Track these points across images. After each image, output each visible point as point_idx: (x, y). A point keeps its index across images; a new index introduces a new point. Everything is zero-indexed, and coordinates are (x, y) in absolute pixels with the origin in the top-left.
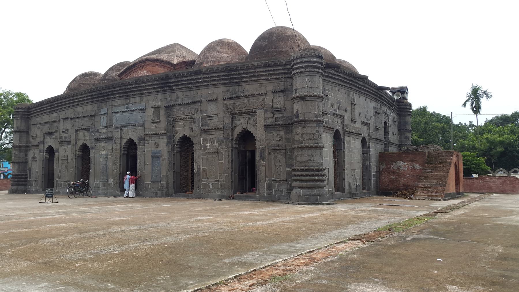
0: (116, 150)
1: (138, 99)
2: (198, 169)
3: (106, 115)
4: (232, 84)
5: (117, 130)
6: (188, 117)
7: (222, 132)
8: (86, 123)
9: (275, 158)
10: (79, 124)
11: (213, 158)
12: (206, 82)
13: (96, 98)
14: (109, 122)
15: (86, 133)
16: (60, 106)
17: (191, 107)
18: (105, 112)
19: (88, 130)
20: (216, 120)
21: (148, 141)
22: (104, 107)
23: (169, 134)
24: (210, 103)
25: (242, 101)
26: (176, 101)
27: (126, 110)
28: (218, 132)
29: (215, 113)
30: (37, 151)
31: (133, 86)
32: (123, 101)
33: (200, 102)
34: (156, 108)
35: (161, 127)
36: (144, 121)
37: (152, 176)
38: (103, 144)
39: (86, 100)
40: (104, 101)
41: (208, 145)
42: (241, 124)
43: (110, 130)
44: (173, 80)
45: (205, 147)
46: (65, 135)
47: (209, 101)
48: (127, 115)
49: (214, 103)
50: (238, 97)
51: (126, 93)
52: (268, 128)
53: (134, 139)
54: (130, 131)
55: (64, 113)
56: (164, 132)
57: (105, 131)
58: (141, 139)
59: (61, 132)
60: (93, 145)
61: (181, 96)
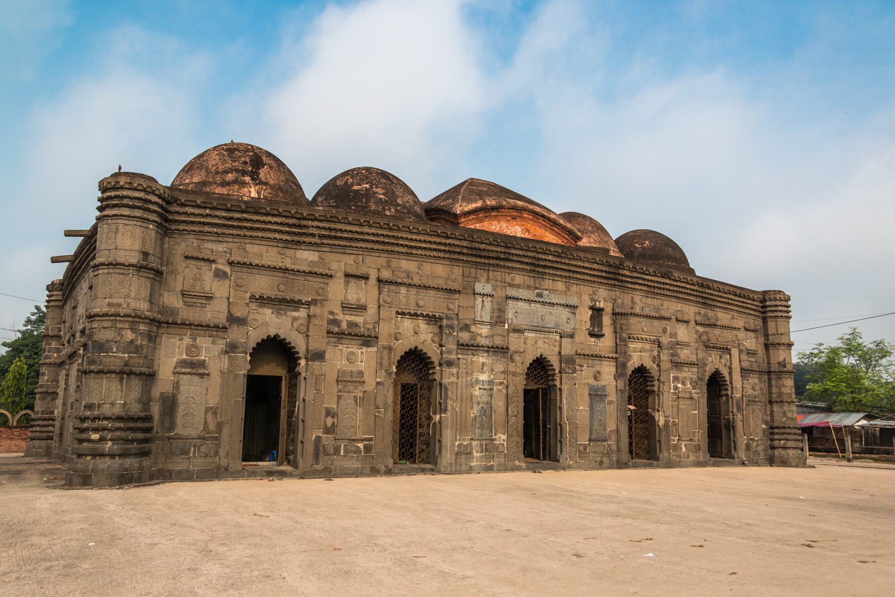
0: (514, 374)
1: (560, 285)
2: (667, 422)
3: (489, 299)
5: (516, 335)
6: (652, 338)
7: (696, 370)
8: (432, 303)
9: (753, 411)
11: (679, 406)
13: (463, 254)
14: (496, 314)
15: (422, 325)
16: (340, 238)
17: (656, 323)
18: (488, 289)
20: (688, 352)
21: (581, 366)
23: (621, 359)
24: (680, 324)
25: (717, 331)
26: (632, 308)
27: (541, 300)
28: (692, 369)
29: (686, 339)
30: (209, 350)
31: (550, 257)
32: (531, 282)
33: (668, 319)
35: (606, 344)
37: (591, 433)
38: (481, 360)
40: (485, 267)
41: (679, 385)
42: (714, 362)
44: (628, 273)
45: (676, 388)
47: (677, 320)
50: (714, 326)
51: (538, 266)
52: (745, 372)
53: (549, 358)
54: (540, 343)
55: (350, 259)
56: (611, 355)
57: (485, 330)
58: (569, 361)
59: (337, 310)
60: (453, 356)
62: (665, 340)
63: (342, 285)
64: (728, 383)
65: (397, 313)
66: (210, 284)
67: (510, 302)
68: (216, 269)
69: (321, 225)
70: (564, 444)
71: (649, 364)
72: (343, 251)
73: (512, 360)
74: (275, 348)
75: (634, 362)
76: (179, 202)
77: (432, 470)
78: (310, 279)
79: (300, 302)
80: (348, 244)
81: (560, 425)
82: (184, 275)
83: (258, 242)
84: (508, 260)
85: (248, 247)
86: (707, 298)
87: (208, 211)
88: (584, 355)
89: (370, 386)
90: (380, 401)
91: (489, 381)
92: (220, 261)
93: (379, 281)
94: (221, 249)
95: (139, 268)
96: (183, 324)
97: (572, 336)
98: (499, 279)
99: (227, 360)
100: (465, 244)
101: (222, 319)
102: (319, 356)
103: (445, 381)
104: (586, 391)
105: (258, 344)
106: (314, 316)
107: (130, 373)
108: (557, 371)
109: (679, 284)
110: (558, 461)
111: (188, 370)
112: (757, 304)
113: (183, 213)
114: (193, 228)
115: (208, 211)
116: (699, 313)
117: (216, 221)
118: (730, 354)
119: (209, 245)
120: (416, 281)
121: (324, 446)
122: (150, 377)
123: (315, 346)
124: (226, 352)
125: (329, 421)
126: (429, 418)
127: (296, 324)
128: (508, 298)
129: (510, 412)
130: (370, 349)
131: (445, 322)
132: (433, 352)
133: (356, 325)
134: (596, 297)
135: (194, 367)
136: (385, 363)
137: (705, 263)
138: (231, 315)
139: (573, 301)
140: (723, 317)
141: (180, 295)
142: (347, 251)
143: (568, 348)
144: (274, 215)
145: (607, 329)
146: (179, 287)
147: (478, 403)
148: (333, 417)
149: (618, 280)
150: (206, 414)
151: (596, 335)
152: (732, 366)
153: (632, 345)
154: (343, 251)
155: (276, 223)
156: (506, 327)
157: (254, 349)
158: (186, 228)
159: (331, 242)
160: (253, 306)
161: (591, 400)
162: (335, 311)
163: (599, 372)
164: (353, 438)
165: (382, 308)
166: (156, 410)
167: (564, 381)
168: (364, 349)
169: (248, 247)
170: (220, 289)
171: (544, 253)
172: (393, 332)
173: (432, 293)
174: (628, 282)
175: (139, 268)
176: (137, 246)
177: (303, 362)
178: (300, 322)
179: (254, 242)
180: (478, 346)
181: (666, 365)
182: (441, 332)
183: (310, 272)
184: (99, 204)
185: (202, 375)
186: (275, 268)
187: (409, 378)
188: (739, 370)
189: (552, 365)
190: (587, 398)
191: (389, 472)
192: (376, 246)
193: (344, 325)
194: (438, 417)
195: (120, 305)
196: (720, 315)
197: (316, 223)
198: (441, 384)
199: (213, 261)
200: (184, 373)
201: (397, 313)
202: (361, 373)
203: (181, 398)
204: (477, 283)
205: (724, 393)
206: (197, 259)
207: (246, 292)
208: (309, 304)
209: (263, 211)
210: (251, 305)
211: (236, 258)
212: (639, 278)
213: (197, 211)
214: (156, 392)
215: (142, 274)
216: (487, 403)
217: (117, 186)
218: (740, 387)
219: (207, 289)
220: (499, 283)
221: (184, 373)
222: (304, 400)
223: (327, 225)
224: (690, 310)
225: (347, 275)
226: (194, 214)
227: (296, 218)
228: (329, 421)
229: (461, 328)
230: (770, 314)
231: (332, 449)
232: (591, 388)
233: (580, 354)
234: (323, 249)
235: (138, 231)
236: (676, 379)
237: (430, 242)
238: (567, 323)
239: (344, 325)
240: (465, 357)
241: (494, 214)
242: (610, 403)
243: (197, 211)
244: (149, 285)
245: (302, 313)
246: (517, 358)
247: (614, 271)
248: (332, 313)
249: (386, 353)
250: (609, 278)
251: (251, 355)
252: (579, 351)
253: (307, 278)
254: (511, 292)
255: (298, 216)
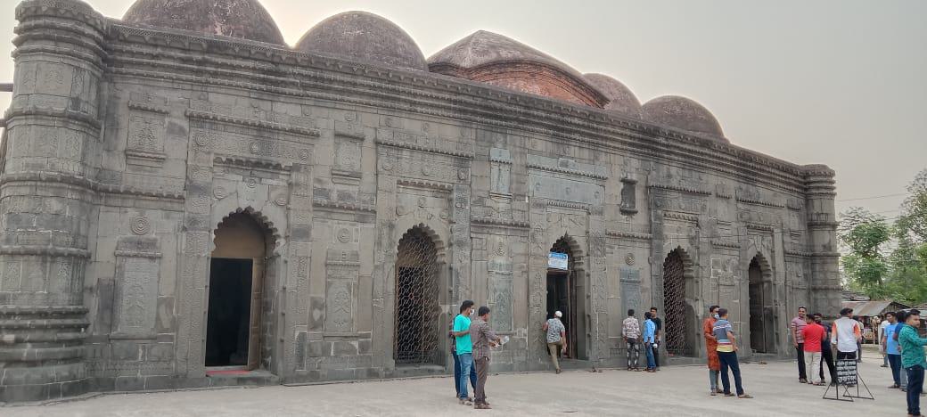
0: (536, 257)
3: (507, 167)
4: (748, 180)
5: (537, 211)
6: (690, 216)
7: (737, 253)
8: (442, 172)
10: (410, 165)
12: (717, 164)
19: (443, 191)
22: (500, 145)
24: (720, 201)
25: (760, 209)
27: (566, 170)
28: (733, 253)
30: (161, 225)
33: (708, 194)
34: (629, 184)
35: (638, 223)
36: (602, 204)
39: (438, 107)
41: (720, 271)
42: (756, 245)
43: (516, 204)
45: (716, 274)
46: (340, 187)
48: (566, 182)
49: (725, 203)
53: (575, 238)
54: (565, 220)
56: (645, 235)
57: (502, 204)
58: (597, 242)
61: (674, 174)
62: (703, 219)
63: (332, 148)
64: (770, 268)
65: (399, 183)
66: (161, 140)
67: (531, 171)
68: (170, 123)
69: (304, 72)
70: (593, 339)
71: (685, 246)
72: (333, 105)
73: (534, 240)
74: (246, 223)
75: (669, 246)
76: (121, 38)
77: (442, 372)
78: (291, 138)
79: (278, 167)
80: (338, 97)
81: (589, 316)
82: (130, 130)
83: (223, 91)
84: (528, 122)
85: (212, 97)
86: (749, 172)
87: (159, 50)
88: (615, 235)
89: (367, 269)
90: (379, 288)
91: (507, 265)
92: (175, 113)
93: (377, 143)
94: (176, 99)
95: (67, 118)
96: (127, 192)
97: (601, 213)
98: (518, 144)
99: (184, 240)
100: (479, 101)
101: (178, 189)
102: (303, 233)
103: (456, 265)
104: (617, 278)
105: (225, 219)
106: (297, 184)
107: (56, 255)
108: (584, 254)
109: (719, 154)
110: (587, 359)
111: (134, 252)
112: (800, 179)
113: (127, 52)
114: (140, 71)
115: (159, 50)
116: (741, 189)
117: (170, 63)
118: (773, 236)
119: (162, 93)
120: (421, 144)
121: (310, 345)
122: (81, 260)
123: (295, 221)
124: (185, 229)
125: (317, 314)
126: (437, 309)
127: (273, 195)
128: (528, 167)
129: (531, 301)
130: (366, 226)
131: (455, 195)
132: (439, 228)
133: (350, 196)
134: (628, 169)
135: (143, 248)
136: (385, 242)
137: (738, 133)
138: (191, 182)
139: (602, 171)
140: (764, 193)
141: (122, 156)
142: (338, 106)
143: (597, 226)
144: (245, 58)
145: (640, 205)
146: (122, 147)
147: (495, 291)
148: (321, 309)
149: (653, 149)
150: (158, 307)
151: (629, 213)
152: (775, 251)
153: (666, 224)
154: (333, 105)
155: (247, 68)
156: (527, 201)
157: (219, 225)
158: (131, 70)
159: (317, 94)
160: (219, 170)
161: (623, 287)
162: (325, 179)
163: (632, 255)
164: (345, 334)
165: (380, 176)
166: (93, 303)
167: (592, 265)
168: (360, 226)
169: (212, 97)
170: (176, 149)
171: (570, 116)
172: (394, 205)
173: (440, 158)
174: (663, 151)
175: (67, 118)
176: (66, 91)
177: (281, 242)
178: (279, 191)
179: (219, 91)
180: (494, 223)
181: (705, 248)
182: (451, 207)
183: (291, 131)
184: (16, 36)
185: (152, 258)
186: (246, 124)
187: (412, 262)
188: (781, 254)
189: (578, 246)
190: (618, 284)
191: (390, 376)
192: (373, 101)
193: (334, 196)
194: (448, 307)
195: (41, 166)
196: (761, 190)
197: (297, 70)
198: (451, 268)
199: (166, 113)
200: (129, 256)
201: (399, 183)
202: (356, 255)
203: (126, 287)
204: (493, 149)
205: (765, 279)
206: (145, 110)
207: (209, 153)
208: (290, 169)
209: (230, 52)
210: (215, 169)
211: (197, 109)
212: (675, 147)
213: (145, 50)
214: (91, 280)
215: (71, 126)
216: (506, 290)
217: (39, 13)
218: (782, 272)
219: (159, 148)
220: (518, 149)
221: (129, 256)
222: (284, 288)
223: (312, 73)
224: (731, 185)
225: (338, 135)
226: (142, 53)
227: (273, 63)
228: (317, 314)
229: (474, 202)
230: (814, 191)
231: (320, 349)
232: (622, 273)
233: (610, 234)
234: (307, 103)
235: (68, 73)
236: (716, 263)
237: (437, 98)
238: (596, 197)
239: (334, 196)
240: (480, 236)
241: (510, 69)
242: (644, 290)
243: (145, 50)
244: (81, 141)
245: (280, 182)
246: (539, 237)
247: (648, 137)
248: (319, 181)
249: (385, 231)
250: (642, 147)
251: (216, 232)
252: (609, 230)
253: (287, 137)
254: (532, 160)
255: (276, 60)
